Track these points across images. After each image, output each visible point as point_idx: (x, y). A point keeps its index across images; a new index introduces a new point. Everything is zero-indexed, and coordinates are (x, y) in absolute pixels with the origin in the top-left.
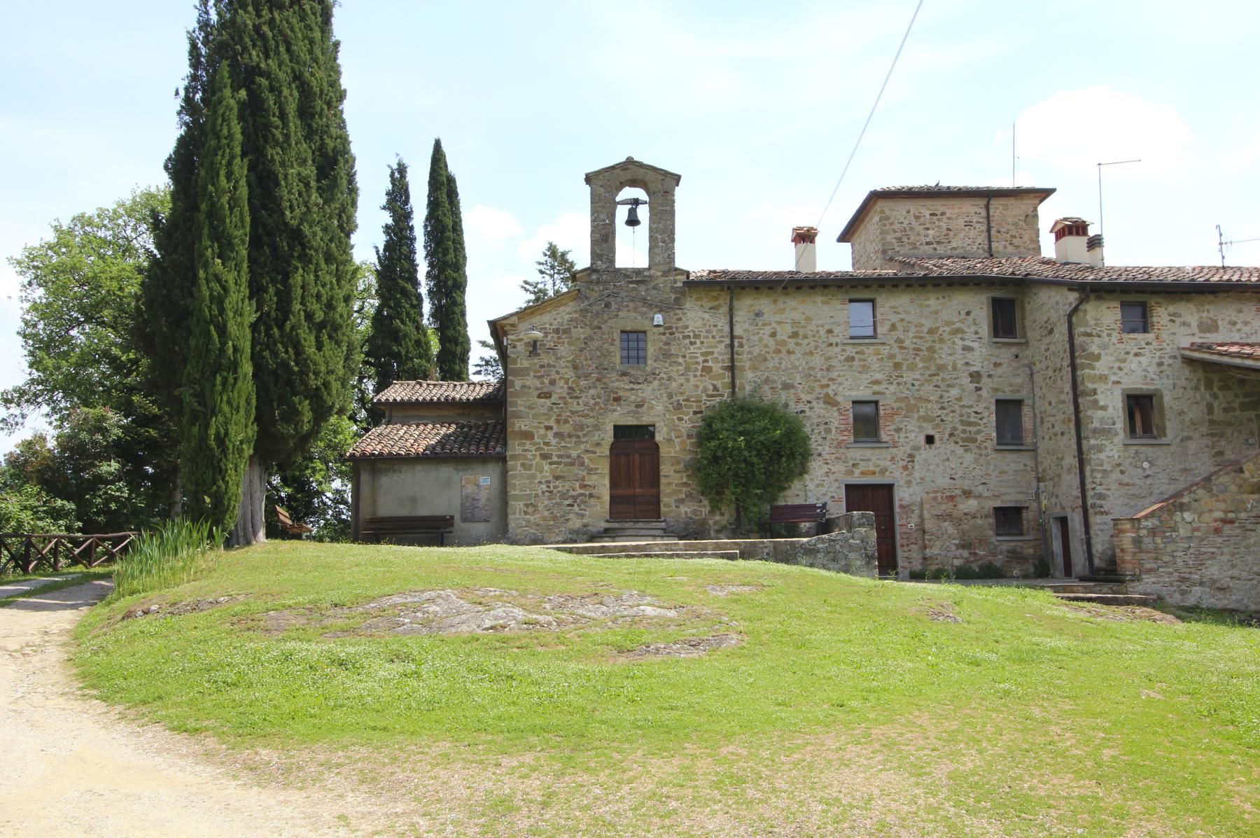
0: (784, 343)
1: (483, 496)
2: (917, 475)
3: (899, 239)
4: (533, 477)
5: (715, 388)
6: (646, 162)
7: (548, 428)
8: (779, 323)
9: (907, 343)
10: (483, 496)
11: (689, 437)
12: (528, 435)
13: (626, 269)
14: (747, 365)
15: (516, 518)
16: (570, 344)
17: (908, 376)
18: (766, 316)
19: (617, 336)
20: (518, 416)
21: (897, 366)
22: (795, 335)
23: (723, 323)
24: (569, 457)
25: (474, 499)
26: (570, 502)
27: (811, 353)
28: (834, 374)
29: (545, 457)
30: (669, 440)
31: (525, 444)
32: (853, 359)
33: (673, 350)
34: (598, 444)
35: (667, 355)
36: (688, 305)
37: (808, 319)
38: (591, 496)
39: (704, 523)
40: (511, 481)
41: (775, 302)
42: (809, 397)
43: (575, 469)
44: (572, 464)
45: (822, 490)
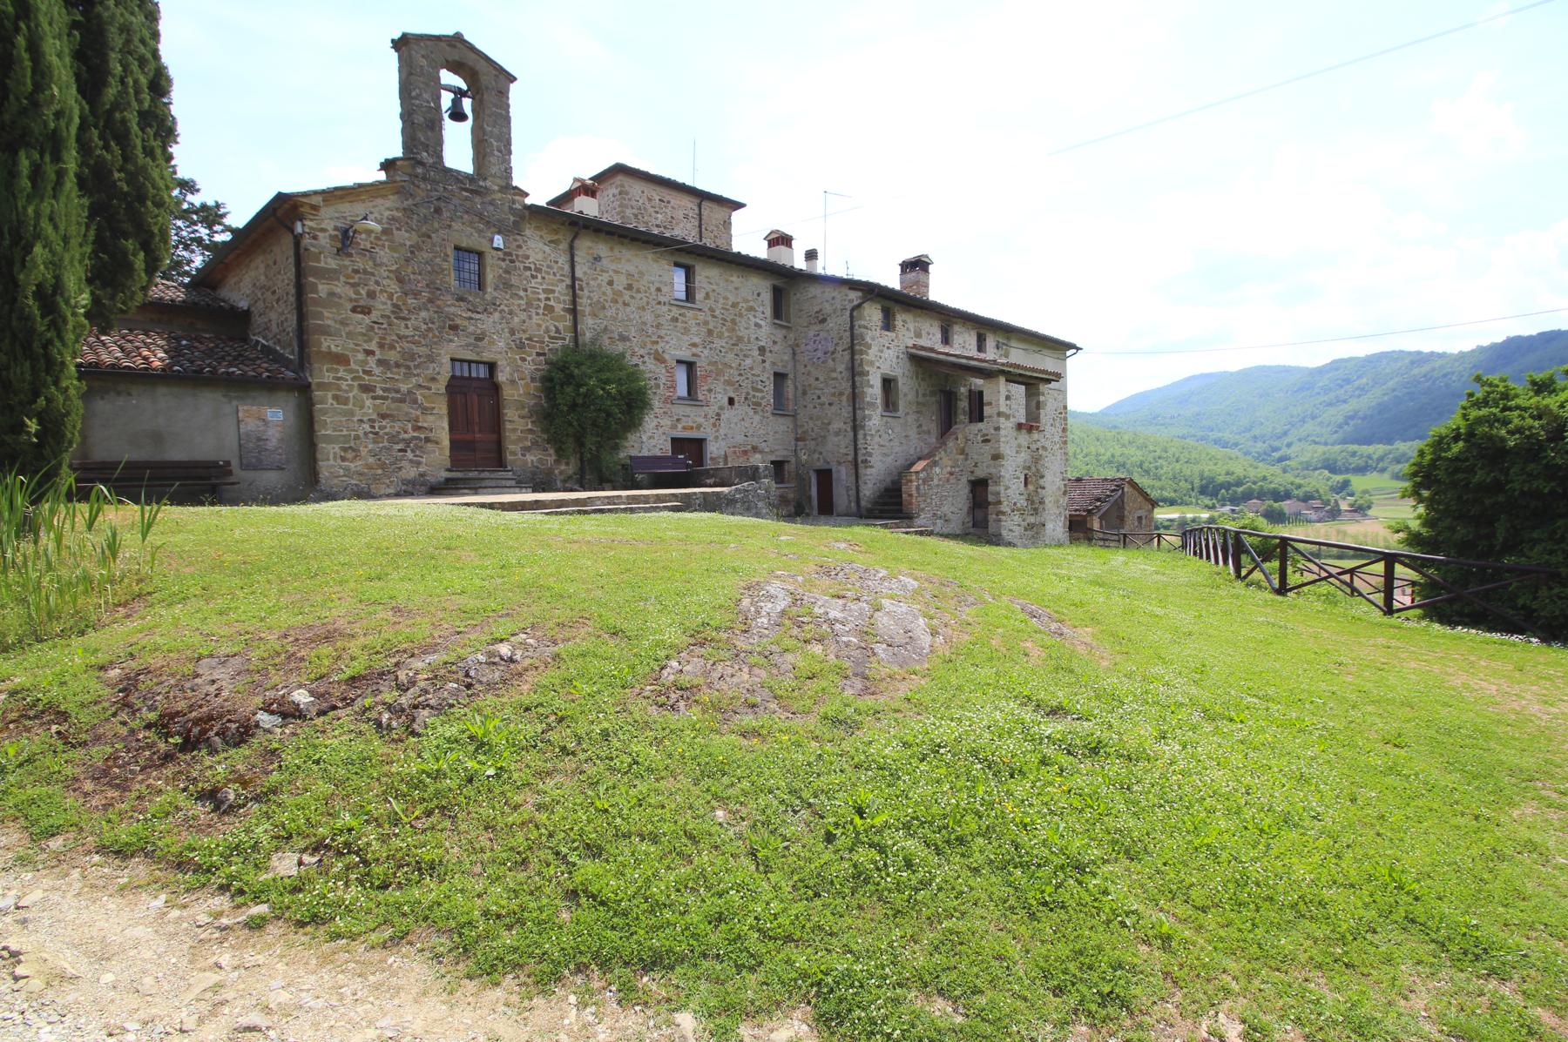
0: (619, 293)
1: (274, 436)
2: (722, 431)
3: (636, 216)
4: (352, 413)
5: (558, 331)
6: (478, 46)
7: (370, 353)
8: (616, 272)
9: (717, 313)
10: (274, 436)
11: (533, 380)
12: (341, 359)
13: (458, 172)
14: (588, 310)
15: (330, 465)
16: (392, 249)
17: (718, 343)
18: (604, 262)
19: (450, 251)
20: (325, 331)
21: (710, 332)
22: (629, 287)
23: (563, 260)
24: (398, 391)
25: (259, 439)
26: (400, 446)
27: (643, 309)
28: (662, 333)
29: (366, 389)
30: (513, 382)
31: (337, 371)
32: (676, 320)
33: (514, 280)
34: (433, 379)
35: (507, 286)
36: (528, 232)
37: (641, 274)
38: (427, 440)
39: (550, 472)
40: (318, 417)
41: (612, 249)
42: (642, 352)
43: (405, 407)
44: (402, 401)
45: (653, 442)
